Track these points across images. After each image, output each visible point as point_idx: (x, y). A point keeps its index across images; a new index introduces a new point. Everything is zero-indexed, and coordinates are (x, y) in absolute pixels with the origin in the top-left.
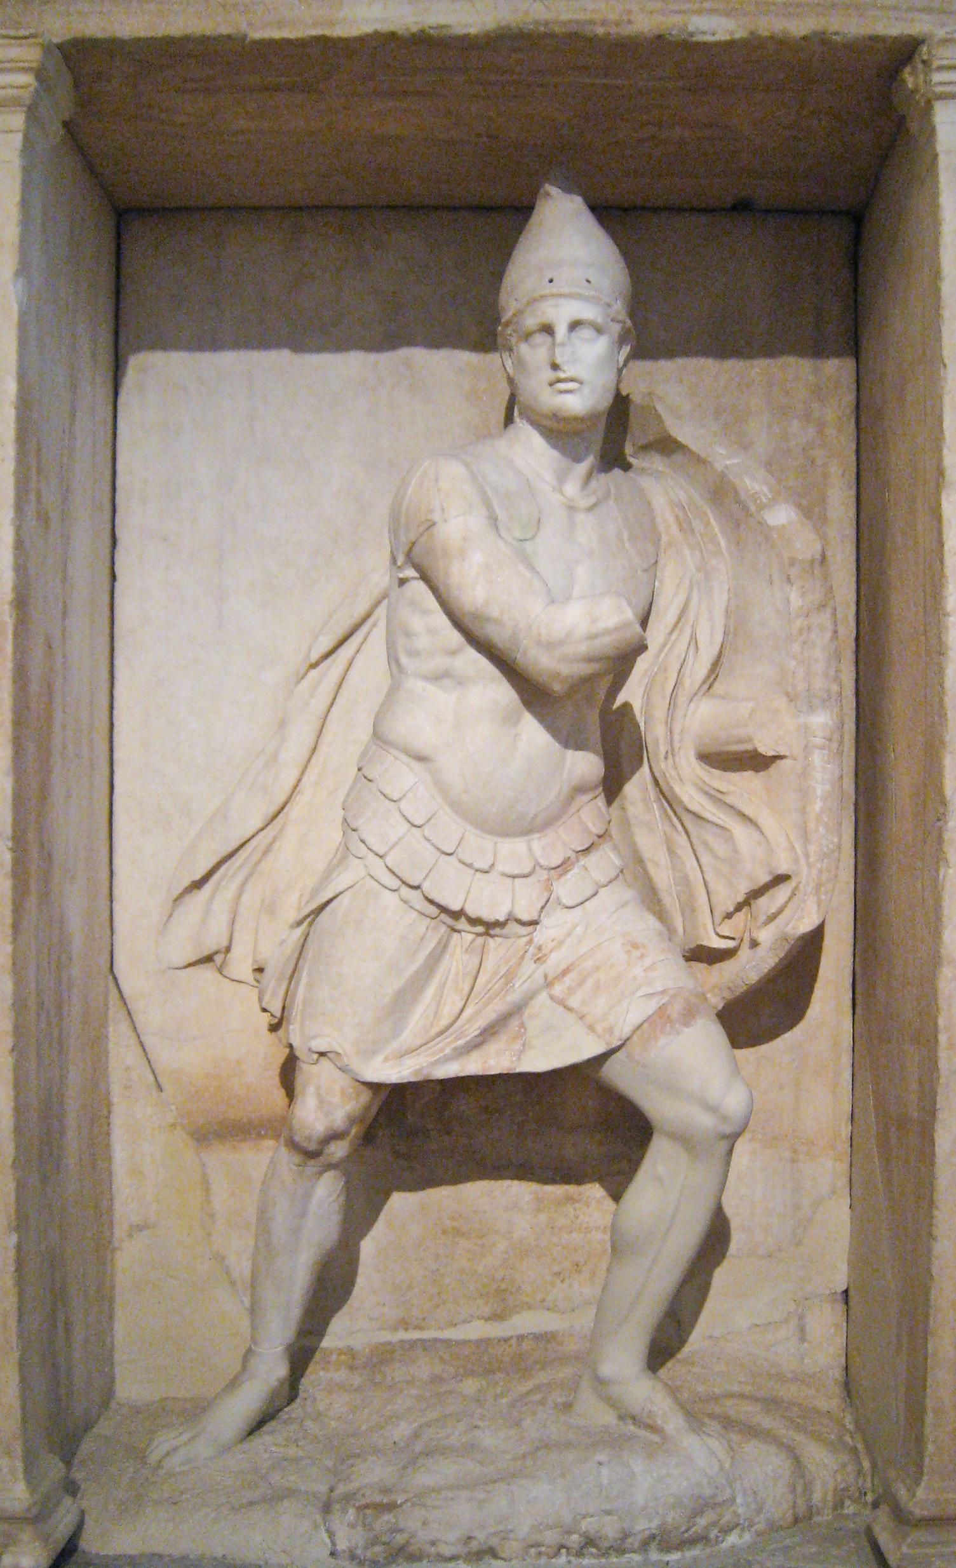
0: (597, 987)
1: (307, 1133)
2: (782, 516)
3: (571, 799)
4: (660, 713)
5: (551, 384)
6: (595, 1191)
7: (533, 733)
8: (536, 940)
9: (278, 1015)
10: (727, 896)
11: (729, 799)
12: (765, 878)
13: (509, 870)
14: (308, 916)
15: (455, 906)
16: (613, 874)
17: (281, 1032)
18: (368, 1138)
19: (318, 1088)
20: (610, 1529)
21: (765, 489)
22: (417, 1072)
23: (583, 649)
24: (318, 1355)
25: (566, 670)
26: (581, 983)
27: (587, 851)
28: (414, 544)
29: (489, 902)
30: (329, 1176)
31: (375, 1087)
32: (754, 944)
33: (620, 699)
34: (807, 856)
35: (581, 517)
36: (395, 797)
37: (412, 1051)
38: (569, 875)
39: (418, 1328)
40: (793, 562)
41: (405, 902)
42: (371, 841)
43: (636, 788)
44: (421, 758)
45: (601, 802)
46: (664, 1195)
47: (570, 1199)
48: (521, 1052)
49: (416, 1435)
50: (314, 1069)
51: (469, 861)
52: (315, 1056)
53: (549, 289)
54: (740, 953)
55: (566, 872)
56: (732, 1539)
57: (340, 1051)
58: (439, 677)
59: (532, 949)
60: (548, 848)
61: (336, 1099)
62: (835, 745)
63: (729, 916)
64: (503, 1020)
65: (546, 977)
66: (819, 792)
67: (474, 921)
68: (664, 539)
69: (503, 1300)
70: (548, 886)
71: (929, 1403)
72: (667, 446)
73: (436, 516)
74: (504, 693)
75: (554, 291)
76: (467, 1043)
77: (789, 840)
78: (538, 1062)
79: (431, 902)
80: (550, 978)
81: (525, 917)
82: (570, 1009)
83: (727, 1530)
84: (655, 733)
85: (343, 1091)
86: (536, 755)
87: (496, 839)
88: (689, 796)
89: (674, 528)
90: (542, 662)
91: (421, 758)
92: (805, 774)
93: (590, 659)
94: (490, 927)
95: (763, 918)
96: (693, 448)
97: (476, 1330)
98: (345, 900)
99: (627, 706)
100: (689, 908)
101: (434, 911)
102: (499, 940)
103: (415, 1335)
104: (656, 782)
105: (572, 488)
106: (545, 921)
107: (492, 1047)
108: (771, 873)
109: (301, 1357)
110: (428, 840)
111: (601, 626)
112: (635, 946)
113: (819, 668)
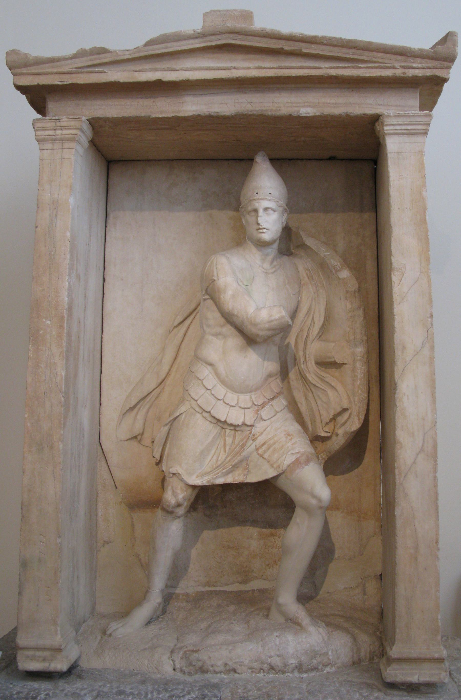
0: (275, 450)
1: (168, 504)
2: (345, 274)
3: (266, 380)
5: (257, 230)
8: (253, 432)
9: (159, 459)
10: (326, 417)
11: (327, 380)
12: (339, 410)
13: (242, 406)
14: (169, 422)
15: (223, 419)
16: (283, 408)
17: (160, 466)
19: (172, 487)
21: (339, 264)
22: (208, 481)
23: (267, 326)
24: (174, 596)
25: (261, 333)
26: (269, 448)
27: (273, 399)
28: (208, 287)
29: (236, 417)
30: (177, 520)
31: (194, 487)
32: (337, 435)
34: (354, 402)
35: (270, 275)
36: (201, 378)
37: (207, 473)
38: (265, 408)
39: (214, 586)
41: (205, 418)
42: (192, 394)
44: (211, 365)
45: (279, 381)
48: (247, 475)
49: (210, 626)
50: (171, 480)
51: (228, 402)
52: (171, 475)
54: (332, 438)
55: (264, 407)
57: (181, 473)
58: (216, 335)
59: (251, 435)
62: (365, 360)
63: (327, 424)
64: (241, 461)
65: (256, 446)
66: (359, 377)
67: (231, 425)
68: (302, 282)
69: (245, 575)
70: (257, 412)
75: (258, 197)
76: (227, 471)
77: (348, 396)
78: (253, 478)
79: (214, 418)
80: (257, 447)
81: (248, 423)
82: (264, 458)
85: (181, 489)
86: (252, 365)
87: (239, 394)
89: (306, 279)
91: (211, 365)
92: (354, 370)
93: (269, 329)
94: (235, 427)
95: (339, 425)
96: (313, 249)
98: (183, 416)
99: (288, 345)
100: (313, 421)
101: (215, 421)
102: (239, 432)
104: (300, 373)
105: (267, 265)
106: (256, 425)
107: (237, 472)
108: (341, 408)
110: (213, 395)
111: (273, 318)
112: (289, 435)
113: (358, 331)
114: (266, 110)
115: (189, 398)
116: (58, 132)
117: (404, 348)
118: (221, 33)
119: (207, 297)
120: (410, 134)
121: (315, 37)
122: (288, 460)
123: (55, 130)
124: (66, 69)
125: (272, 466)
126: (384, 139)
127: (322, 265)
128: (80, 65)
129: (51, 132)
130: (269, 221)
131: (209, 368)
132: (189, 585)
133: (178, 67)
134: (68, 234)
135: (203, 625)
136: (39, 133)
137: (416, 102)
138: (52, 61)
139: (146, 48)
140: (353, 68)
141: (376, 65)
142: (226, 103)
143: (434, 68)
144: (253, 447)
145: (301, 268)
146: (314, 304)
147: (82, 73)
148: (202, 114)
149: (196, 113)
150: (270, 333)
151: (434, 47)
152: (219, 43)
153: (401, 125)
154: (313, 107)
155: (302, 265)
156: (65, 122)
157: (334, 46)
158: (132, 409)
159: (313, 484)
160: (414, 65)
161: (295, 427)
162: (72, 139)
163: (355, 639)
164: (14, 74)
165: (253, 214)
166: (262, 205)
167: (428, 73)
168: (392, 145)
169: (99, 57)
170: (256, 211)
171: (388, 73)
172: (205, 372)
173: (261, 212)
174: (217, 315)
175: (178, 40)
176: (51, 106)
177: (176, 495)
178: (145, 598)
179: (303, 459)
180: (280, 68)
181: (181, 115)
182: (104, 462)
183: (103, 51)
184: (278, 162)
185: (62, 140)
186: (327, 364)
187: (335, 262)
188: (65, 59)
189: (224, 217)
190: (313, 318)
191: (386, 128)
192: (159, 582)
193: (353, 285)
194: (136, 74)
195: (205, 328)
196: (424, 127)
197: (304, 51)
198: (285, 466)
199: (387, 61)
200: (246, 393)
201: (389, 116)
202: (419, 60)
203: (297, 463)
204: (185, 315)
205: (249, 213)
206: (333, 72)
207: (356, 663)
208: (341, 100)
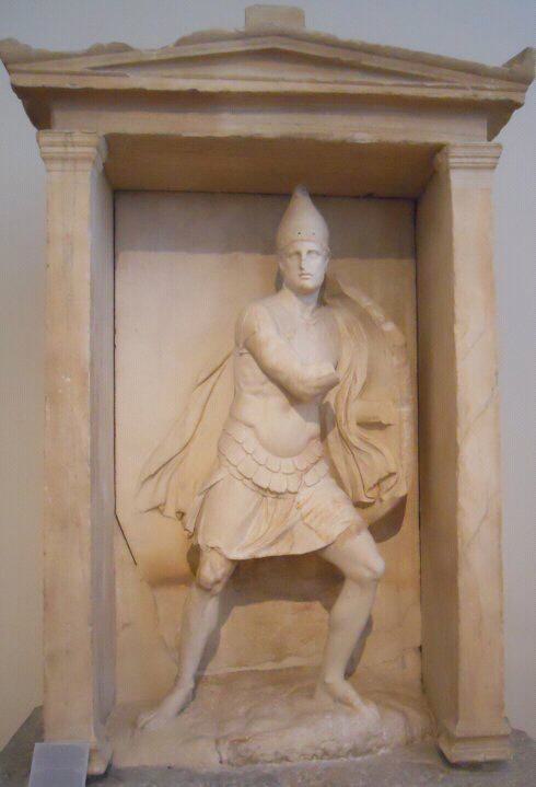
2: (389, 327)
4: (342, 406)
6: (317, 605)
7: (294, 417)
10: (369, 482)
13: (285, 471)
15: (265, 485)
17: (193, 539)
18: (227, 586)
20: (332, 747)
23: (315, 384)
25: (309, 392)
29: (279, 483)
30: (214, 599)
31: (233, 561)
32: (381, 500)
33: (326, 399)
40: (394, 346)
43: (331, 437)
44: (251, 426)
46: (351, 606)
47: (307, 608)
49: (249, 712)
50: (208, 555)
56: (382, 751)
58: (256, 394)
60: (301, 462)
61: (219, 566)
63: (371, 489)
67: (272, 493)
72: (342, 296)
73: (256, 329)
74: (277, 400)
78: (299, 550)
81: (292, 491)
83: (380, 747)
84: (341, 414)
86: (296, 426)
88: (354, 439)
89: (346, 331)
90: (301, 388)
91: (251, 426)
93: (318, 387)
94: (278, 495)
97: (269, 666)
98: (220, 486)
100: (354, 487)
103: (244, 668)
104: (341, 435)
105: (307, 316)
107: (281, 543)
109: (198, 680)
115: (227, 464)
116: (70, 149)
118: (266, 35)
119: (245, 351)
120: (477, 168)
121: (377, 47)
122: (336, 530)
123: (65, 146)
124: (77, 68)
125: (320, 536)
126: (448, 172)
127: (364, 317)
128: (97, 64)
129: (61, 149)
130: (312, 266)
131: (249, 429)
132: (220, 666)
134: (88, 276)
135: (242, 710)
136: (48, 149)
137: (484, 132)
138: (61, 57)
139: (178, 48)
141: (446, 84)
143: (510, 90)
144: (298, 516)
146: (357, 357)
147: (98, 75)
148: (242, 134)
149: (236, 134)
150: (318, 391)
151: (510, 63)
152: (265, 47)
154: (368, 132)
155: (341, 317)
156: (77, 138)
157: (398, 58)
158: (152, 476)
159: (364, 555)
160: (488, 86)
161: (339, 493)
162: (84, 159)
163: (404, 715)
164: (9, 71)
165: (295, 257)
167: (502, 96)
168: (459, 181)
169: (118, 56)
170: (299, 254)
171: (457, 94)
172: (243, 434)
174: (258, 372)
175: (214, 40)
176: (59, 116)
177: (213, 569)
178: (175, 685)
179: (353, 528)
180: (336, 82)
181: (218, 135)
182: (121, 538)
183: (125, 48)
184: (320, 199)
185: (75, 160)
186: (369, 425)
187: (377, 314)
188: (77, 55)
189: (250, 262)
190: (355, 375)
191: (451, 160)
192: (190, 667)
193: (399, 339)
194: (166, 81)
195: (242, 385)
196: (494, 161)
197: (364, 63)
198: (334, 538)
200: (288, 456)
201: (455, 146)
203: (347, 534)
204: (211, 370)
205: (290, 256)
206: (397, 91)
207: (409, 743)
208: (400, 126)
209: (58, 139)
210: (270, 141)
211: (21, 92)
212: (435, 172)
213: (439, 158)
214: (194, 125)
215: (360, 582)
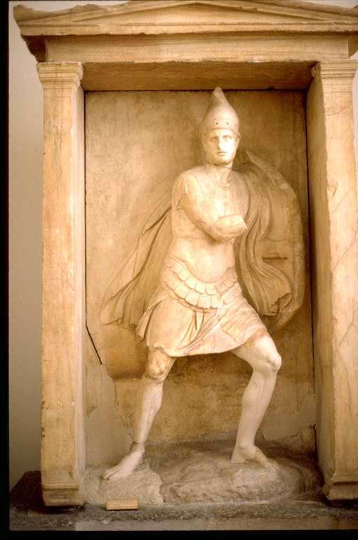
3: (227, 271)
8: (217, 314)
10: (272, 300)
18: (167, 378)
31: (173, 358)
53: (218, 126)
71: (336, 448)
82: (228, 334)
98: (163, 302)
114: (227, 58)
116: (59, 75)
117: (337, 247)
123: (56, 73)
129: (54, 75)
130: (228, 147)
133: (158, 22)
136: (42, 76)
140: (297, 24)
142: (194, 52)
145: (249, 183)
153: (329, 70)
159: (267, 350)
160: (346, 22)
164: (20, 26)
166: (221, 133)
170: (216, 138)
173: (221, 139)
176: (51, 51)
177: (160, 365)
179: (258, 334)
181: (158, 61)
188: (65, 14)
191: (322, 73)
193: (293, 195)
199: (324, 19)
202: (350, 18)
208: (286, 49)
209: (51, 68)
210: (196, 63)
211: (26, 38)
212: (312, 79)
213: (314, 71)
214: (143, 55)
215: (265, 373)
